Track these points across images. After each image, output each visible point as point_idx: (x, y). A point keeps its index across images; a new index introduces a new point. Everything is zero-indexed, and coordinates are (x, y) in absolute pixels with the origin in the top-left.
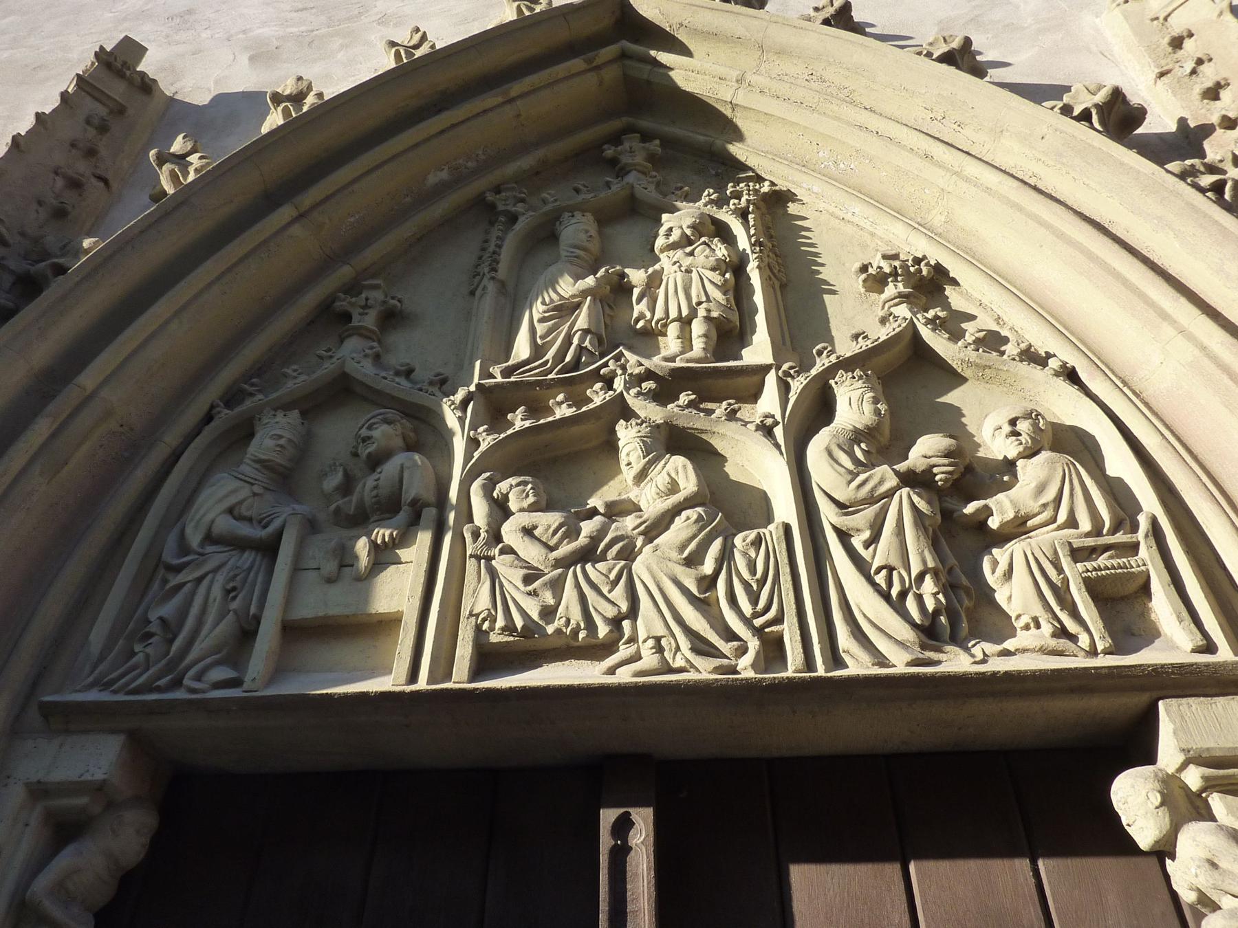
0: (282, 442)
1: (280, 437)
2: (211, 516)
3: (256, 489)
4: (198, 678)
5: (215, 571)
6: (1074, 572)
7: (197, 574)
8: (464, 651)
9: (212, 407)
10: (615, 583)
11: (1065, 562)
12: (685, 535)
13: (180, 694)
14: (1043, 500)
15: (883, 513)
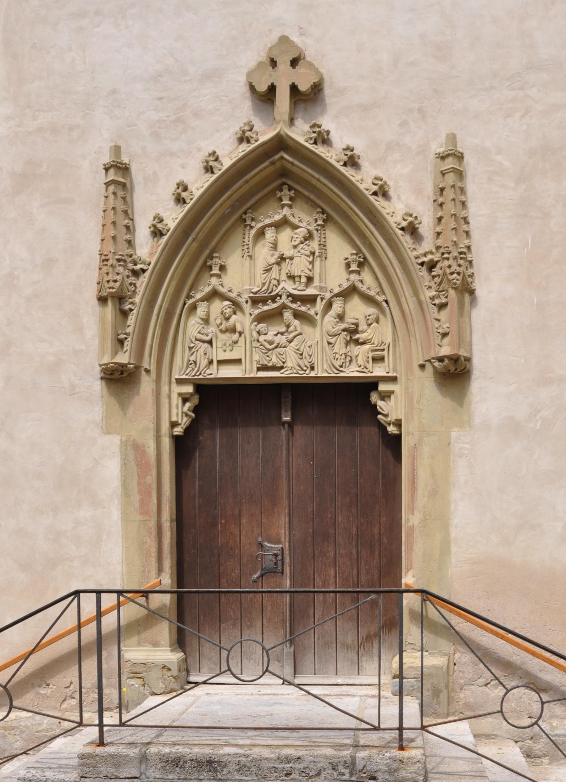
0: (205, 313)
1: (204, 311)
2: (195, 335)
3: (203, 326)
4: (204, 373)
5: (200, 348)
6: (371, 355)
7: (197, 349)
8: (255, 369)
9: (185, 301)
10: (282, 355)
11: (370, 352)
12: (297, 343)
13: (201, 377)
14: (369, 338)
15: (338, 338)
